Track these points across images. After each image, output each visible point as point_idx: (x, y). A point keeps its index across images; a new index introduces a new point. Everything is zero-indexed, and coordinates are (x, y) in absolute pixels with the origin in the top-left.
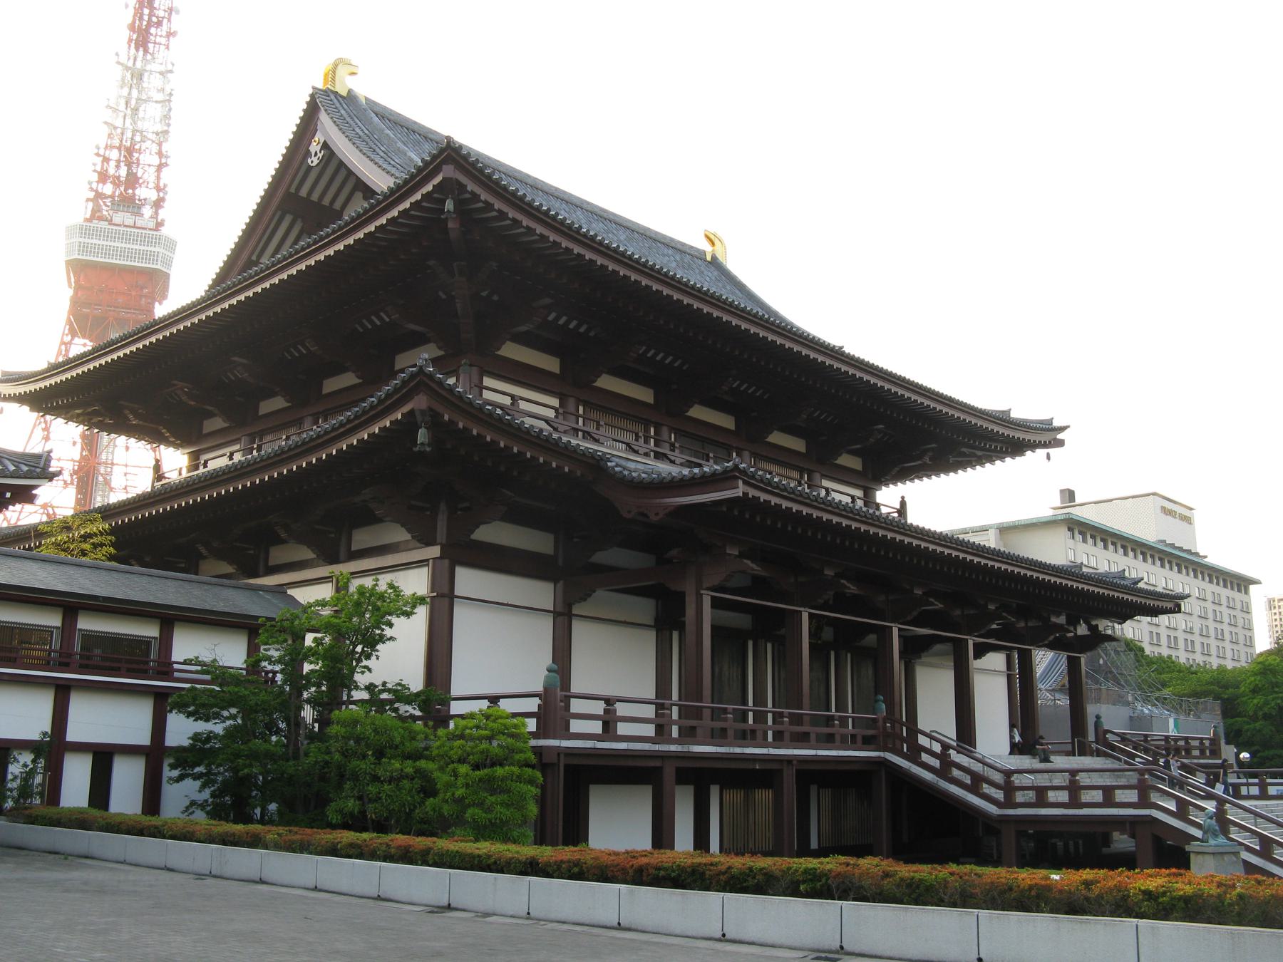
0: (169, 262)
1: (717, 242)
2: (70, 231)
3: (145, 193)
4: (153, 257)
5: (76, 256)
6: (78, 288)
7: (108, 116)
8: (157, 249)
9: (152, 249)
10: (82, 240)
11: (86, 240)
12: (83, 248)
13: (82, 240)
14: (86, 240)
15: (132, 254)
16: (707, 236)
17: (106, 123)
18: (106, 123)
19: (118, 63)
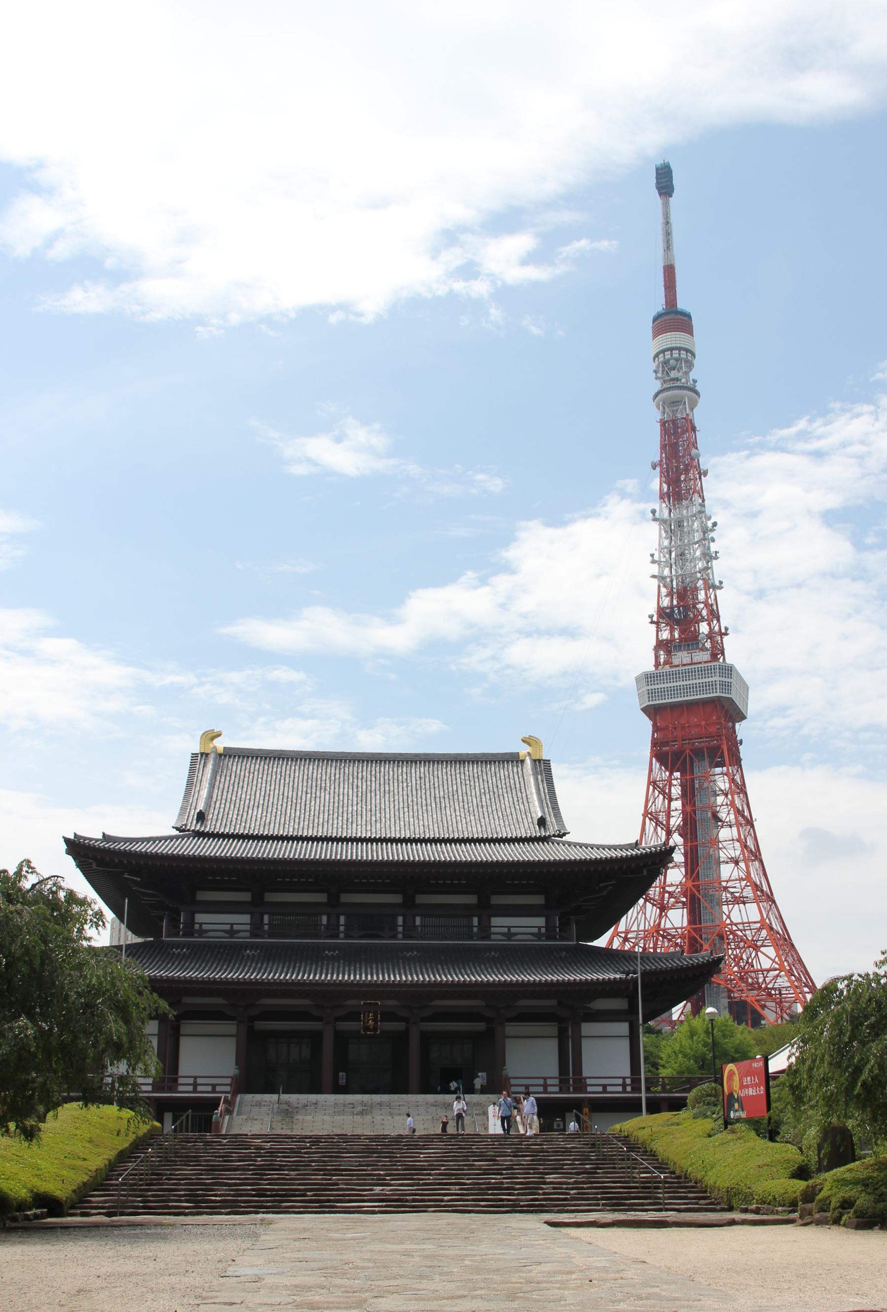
0: (727, 687)
1: (532, 742)
2: (638, 680)
3: (704, 628)
4: (712, 685)
5: (647, 703)
6: (656, 729)
7: (655, 569)
8: (713, 679)
9: (710, 679)
10: (650, 687)
11: (653, 687)
12: (651, 694)
13: (650, 687)
14: (653, 687)
15: (687, 689)
16: (524, 741)
17: (654, 576)
18: (654, 576)
19: (655, 520)
